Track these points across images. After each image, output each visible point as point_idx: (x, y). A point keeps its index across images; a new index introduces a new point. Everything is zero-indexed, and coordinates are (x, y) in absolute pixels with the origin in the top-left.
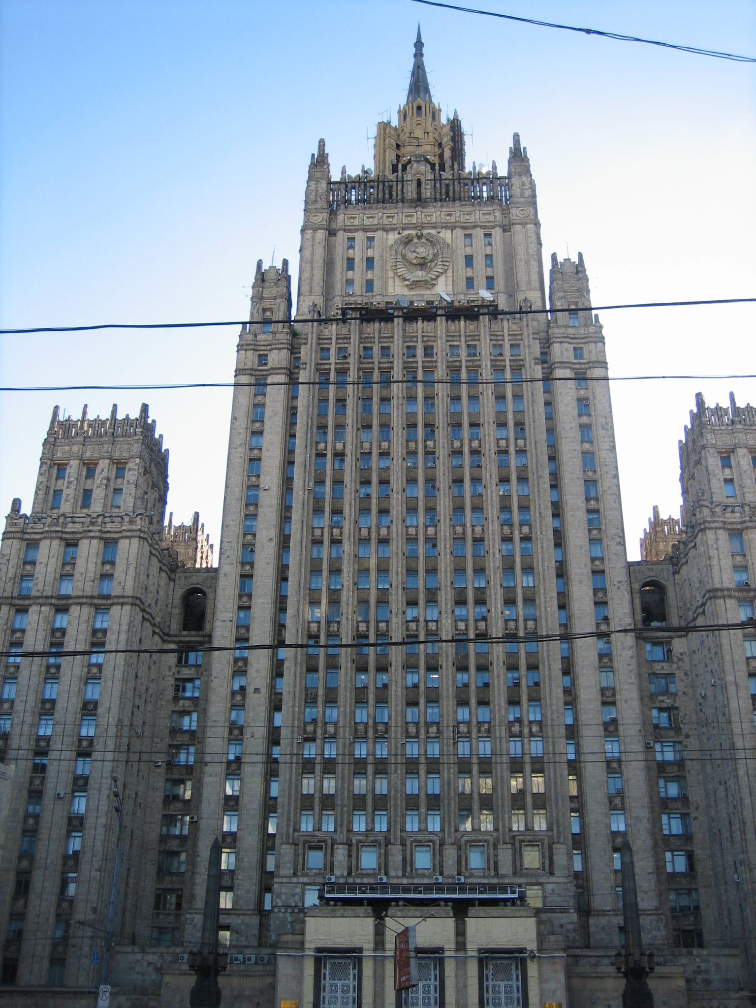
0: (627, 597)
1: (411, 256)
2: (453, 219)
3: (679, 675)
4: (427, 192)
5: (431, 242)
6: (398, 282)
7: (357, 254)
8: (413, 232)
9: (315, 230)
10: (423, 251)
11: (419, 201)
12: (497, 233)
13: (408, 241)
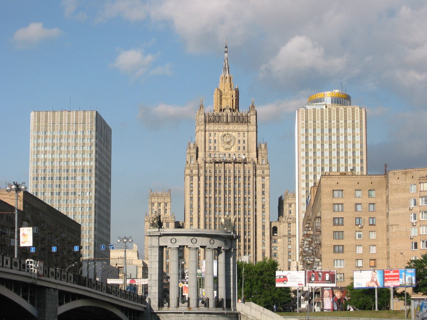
0: (269, 231)
1: (225, 141)
2: (236, 129)
3: (278, 246)
4: (229, 120)
5: (231, 136)
6: (222, 148)
7: (212, 138)
8: (226, 133)
9: (202, 131)
10: (228, 140)
11: (227, 123)
12: (246, 133)
13: (225, 135)
